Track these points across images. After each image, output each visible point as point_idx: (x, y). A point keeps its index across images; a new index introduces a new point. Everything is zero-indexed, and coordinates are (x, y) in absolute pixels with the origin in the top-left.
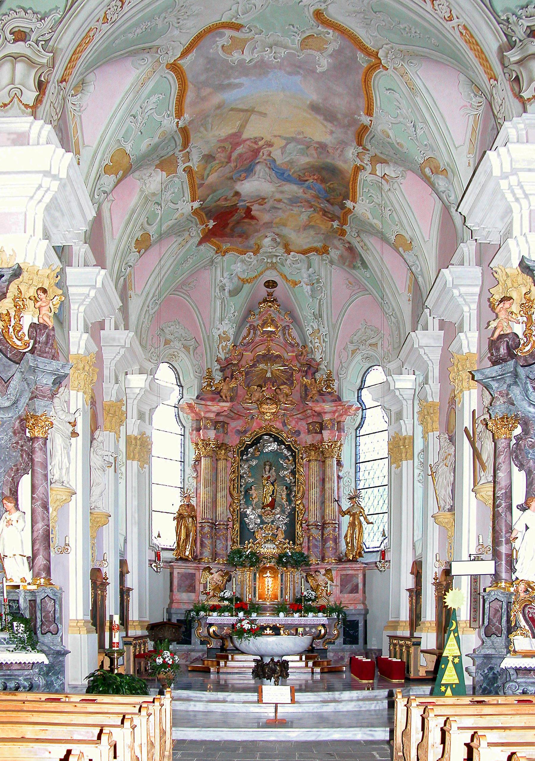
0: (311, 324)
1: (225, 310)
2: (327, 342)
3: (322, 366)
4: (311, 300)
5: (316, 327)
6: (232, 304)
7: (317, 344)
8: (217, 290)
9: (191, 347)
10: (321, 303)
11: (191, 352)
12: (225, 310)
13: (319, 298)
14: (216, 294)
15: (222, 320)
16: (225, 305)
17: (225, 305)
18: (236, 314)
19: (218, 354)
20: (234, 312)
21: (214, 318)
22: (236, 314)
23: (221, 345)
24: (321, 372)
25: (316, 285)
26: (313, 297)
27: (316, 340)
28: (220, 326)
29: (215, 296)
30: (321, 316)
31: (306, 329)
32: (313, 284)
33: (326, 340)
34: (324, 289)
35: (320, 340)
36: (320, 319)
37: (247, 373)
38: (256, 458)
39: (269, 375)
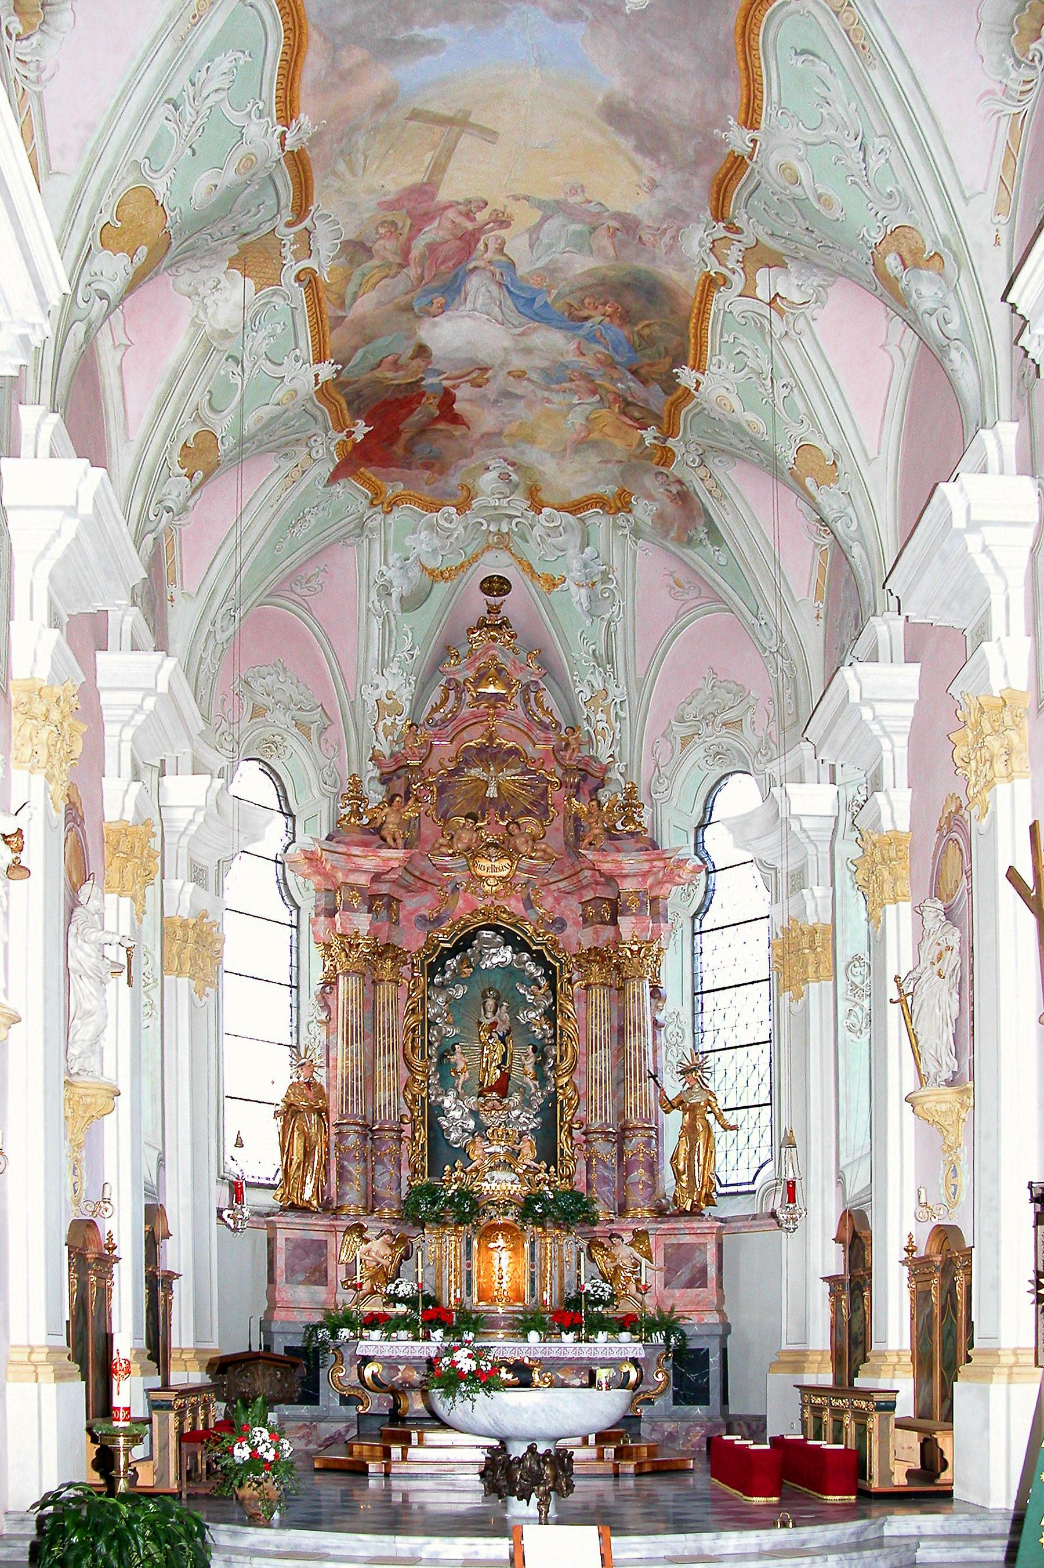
0: (588, 677)
1: (390, 642)
2: (625, 718)
3: (614, 775)
4: (588, 622)
5: (598, 684)
6: (406, 628)
7: (600, 725)
8: (374, 596)
9: (314, 727)
10: (612, 629)
11: (314, 737)
12: (390, 642)
13: (607, 616)
14: (371, 606)
15: (383, 665)
16: (390, 631)
17: (390, 631)
18: (416, 652)
19: (375, 743)
20: (413, 648)
21: (366, 661)
22: (416, 652)
23: (381, 724)
24: (612, 787)
25: (599, 587)
26: (591, 613)
27: (600, 716)
28: (378, 679)
29: (369, 610)
30: (610, 660)
31: (577, 690)
32: (593, 584)
33: (622, 714)
34: (617, 597)
35: (608, 714)
36: (609, 666)
37: (442, 790)
38: (463, 982)
39: (492, 792)
